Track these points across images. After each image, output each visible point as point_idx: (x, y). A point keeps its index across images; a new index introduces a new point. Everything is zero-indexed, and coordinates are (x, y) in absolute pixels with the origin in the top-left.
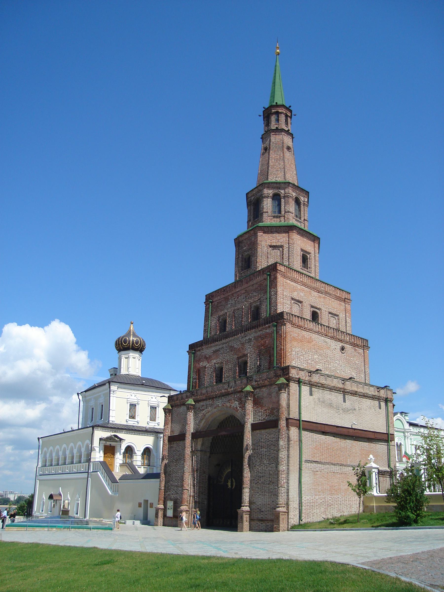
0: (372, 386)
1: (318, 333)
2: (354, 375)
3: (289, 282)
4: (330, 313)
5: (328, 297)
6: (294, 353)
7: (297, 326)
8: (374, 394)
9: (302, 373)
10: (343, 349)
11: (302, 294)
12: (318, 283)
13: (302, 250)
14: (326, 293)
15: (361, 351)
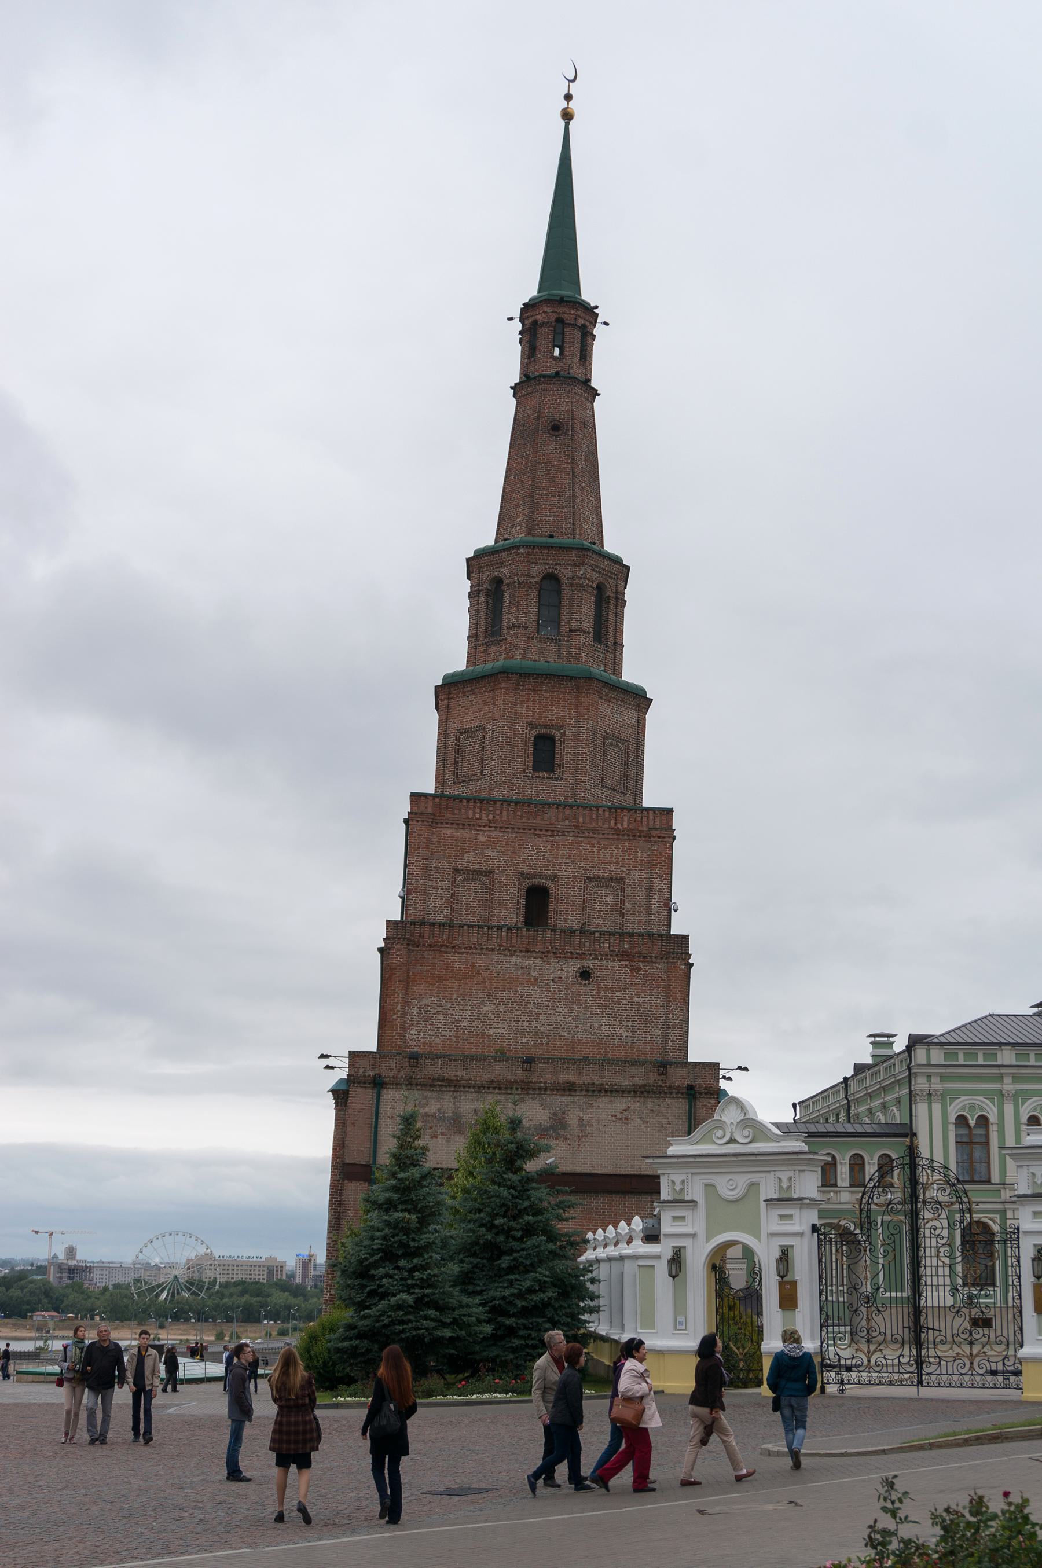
0: (637, 1063)
1: (499, 949)
2: (625, 1034)
3: (448, 832)
4: (588, 878)
5: (586, 841)
6: (415, 1010)
7: (430, 946)
8: (641, 1082)
9: (392, 1063)
10: (585, 974)
11: (492, 854)
12: (552, 813)
13: (532, 725)
14: (579, 830)
15: (658, 969)
